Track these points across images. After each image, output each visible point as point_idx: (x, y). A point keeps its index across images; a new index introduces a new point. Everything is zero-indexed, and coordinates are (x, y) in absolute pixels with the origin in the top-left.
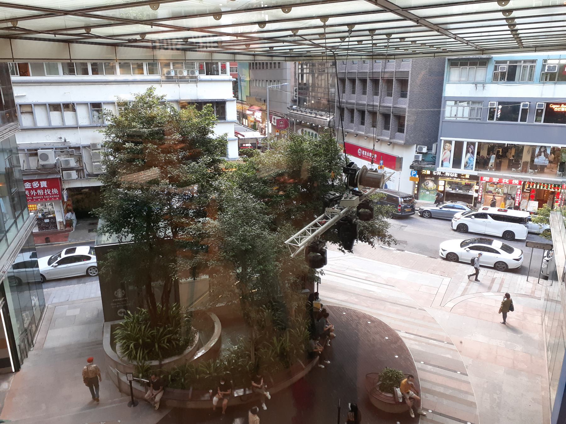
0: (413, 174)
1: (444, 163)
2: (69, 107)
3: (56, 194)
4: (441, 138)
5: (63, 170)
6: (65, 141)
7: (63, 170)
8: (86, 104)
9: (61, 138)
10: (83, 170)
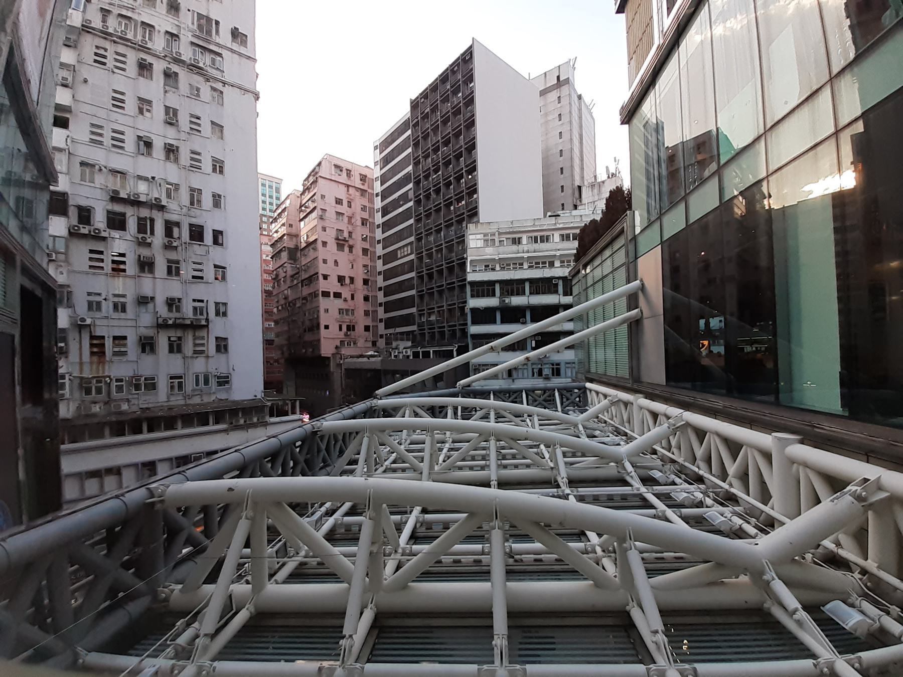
2: (116, 471)
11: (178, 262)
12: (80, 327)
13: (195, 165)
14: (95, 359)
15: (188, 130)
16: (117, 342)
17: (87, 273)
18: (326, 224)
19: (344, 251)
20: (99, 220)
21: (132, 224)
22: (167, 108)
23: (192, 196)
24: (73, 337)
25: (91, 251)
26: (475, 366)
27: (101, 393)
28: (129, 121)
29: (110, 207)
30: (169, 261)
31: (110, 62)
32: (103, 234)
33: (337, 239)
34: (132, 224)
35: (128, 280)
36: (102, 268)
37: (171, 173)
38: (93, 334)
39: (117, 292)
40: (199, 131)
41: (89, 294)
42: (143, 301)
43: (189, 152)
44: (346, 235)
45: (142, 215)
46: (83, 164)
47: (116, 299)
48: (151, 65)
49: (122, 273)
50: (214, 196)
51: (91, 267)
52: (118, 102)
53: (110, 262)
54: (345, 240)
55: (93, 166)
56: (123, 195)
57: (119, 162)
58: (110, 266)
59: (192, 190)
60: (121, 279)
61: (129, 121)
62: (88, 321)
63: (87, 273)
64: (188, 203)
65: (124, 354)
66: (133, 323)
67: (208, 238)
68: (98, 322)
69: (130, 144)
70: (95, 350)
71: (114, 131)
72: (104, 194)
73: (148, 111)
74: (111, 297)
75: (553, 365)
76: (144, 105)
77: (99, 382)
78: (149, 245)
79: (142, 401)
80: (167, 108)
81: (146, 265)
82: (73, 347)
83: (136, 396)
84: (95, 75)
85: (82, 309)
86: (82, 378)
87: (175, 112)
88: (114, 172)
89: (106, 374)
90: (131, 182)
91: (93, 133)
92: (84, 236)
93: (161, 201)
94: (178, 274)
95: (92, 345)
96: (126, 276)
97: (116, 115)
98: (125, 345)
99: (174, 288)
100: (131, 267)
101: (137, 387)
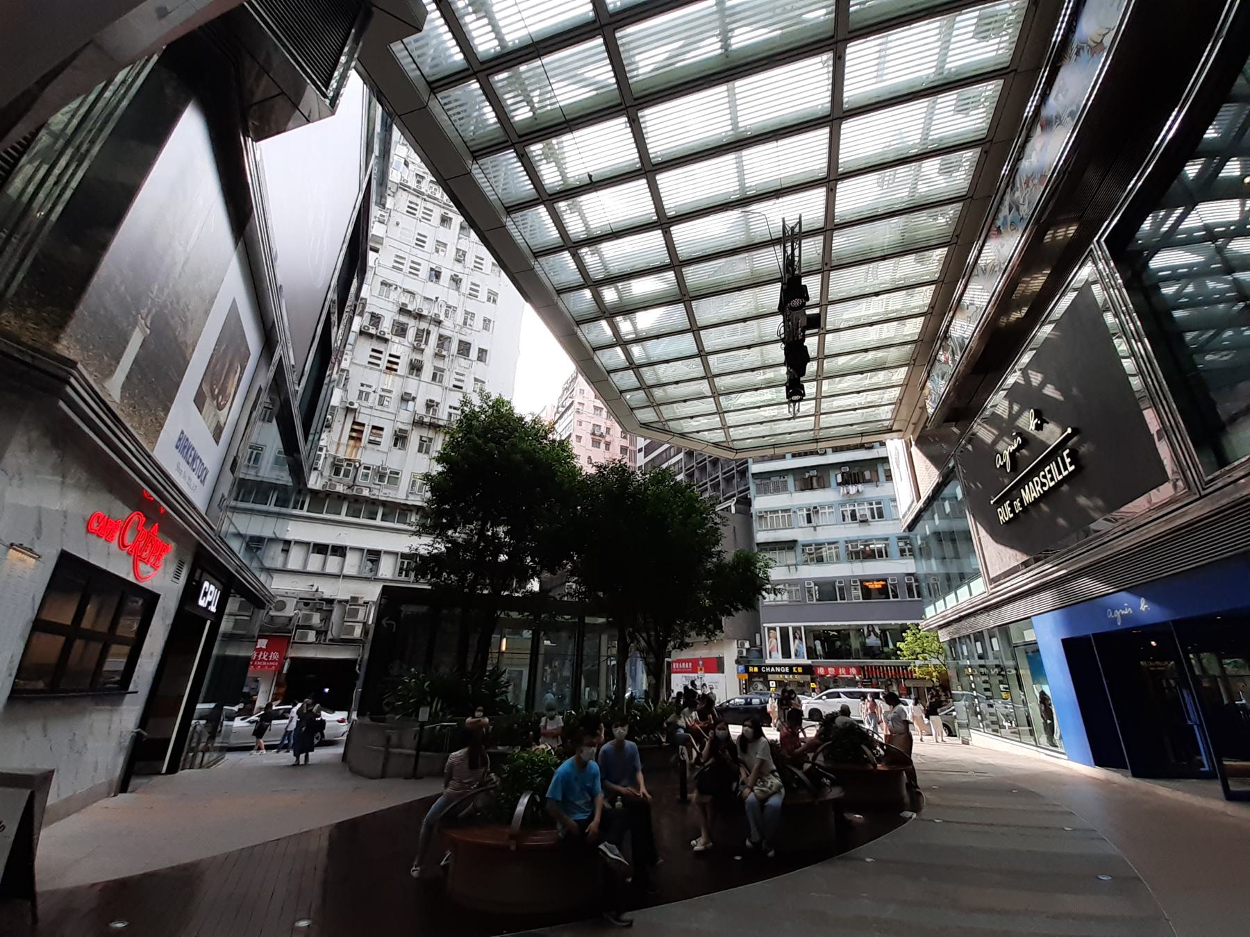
0: (740, 669)
1: (772, 654)
2: (340, 551)
3: (275, 661)
4: (764, 625)
5: (298, 627)
6: (317, 591)
7: (298, 627)
8: (361, 550)
9: (312, 586)
10: (326, 632)
11: (443, 370)
12: (349, 410)
13: (473, 293)
14: (352, 442)
15: (472, 267)
16: (374, 431)
17: (366, 367)
18: (583, 417)
19: (599, 448)
20: (386, 326)
21: (411, 333)
22: (458, 250)
23: (466, 319)
24: (340, 416)
25: (373, 350)
26: (760, 512)
27: (348, 476)
28: (427, 257)
29: (396, 318)
30: (435, 368)
31: (419, 214)
32: (387, 336)
33: (593, 434)
34: (411, 333)
35: (397, 378)
36: (378, 365)
37: (453, 298)
38: (356, 420)
39: (385, 387)
40: (481, 269)
41: (362, 385)
42: (406, 398)
43: (469, 283)
44: (603, 430)
45: (421, 328)
46: (383, 283)
47: (383, 394)
48: (451, 219)
49: (393, 372)
50: (485, 320)
51: (369, 363)
52: (420, 242)
53: (386, 361)
54: (601, 435)
55: (391, 285)
56: (410, 308)
57: (410, 284)
58: (386, 364)
59: (467, 313)
60: (391, 376)
61: (427, 257)
62: (356, 406)
63: (366, 367)
64: (461, 324)
65: (378, 443)
66: (392, 417)
67: (474, 354)
68: (363, 410)
69: (424, 272)
70: (354, 434)
71: (413, 262)
72: (395, 306)
73: (442, 251)
74: (379, 391)
75: (871, 504)
76: (441, 245)
77: (349, 465)
78: (422, 350)
79: (385, 493)
80: (458, 250)
81: (416, 368)
82: (337, 426)
83: (378, 487)
84: (406, 221)
85: (353, 396)
86: (335, 458)
87: (464, 254)
88: (406, 291)
89: (358, 458)
90: (419, 300)
91: (396, 262)
92: (371, 336)
93: (439, 316)
94: (441, 381)
95: (353, 430)
96: (396, 375)
97: (417, 251)
98: (380, 436)
99: (435, 393)
100: (403, 368)
101: (382, 477)
